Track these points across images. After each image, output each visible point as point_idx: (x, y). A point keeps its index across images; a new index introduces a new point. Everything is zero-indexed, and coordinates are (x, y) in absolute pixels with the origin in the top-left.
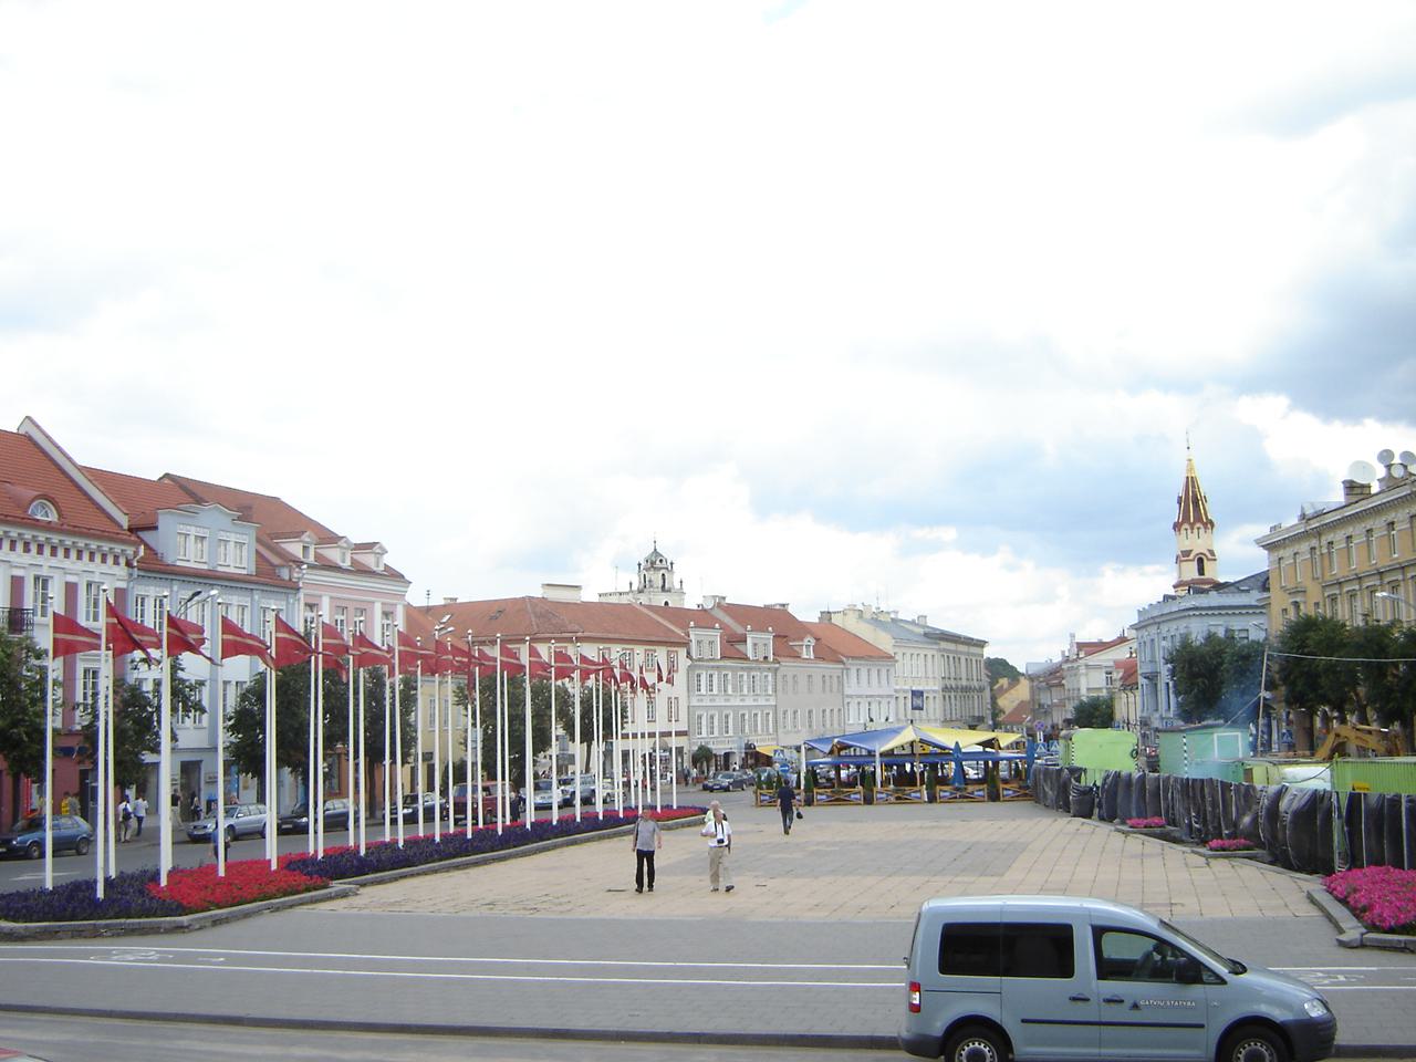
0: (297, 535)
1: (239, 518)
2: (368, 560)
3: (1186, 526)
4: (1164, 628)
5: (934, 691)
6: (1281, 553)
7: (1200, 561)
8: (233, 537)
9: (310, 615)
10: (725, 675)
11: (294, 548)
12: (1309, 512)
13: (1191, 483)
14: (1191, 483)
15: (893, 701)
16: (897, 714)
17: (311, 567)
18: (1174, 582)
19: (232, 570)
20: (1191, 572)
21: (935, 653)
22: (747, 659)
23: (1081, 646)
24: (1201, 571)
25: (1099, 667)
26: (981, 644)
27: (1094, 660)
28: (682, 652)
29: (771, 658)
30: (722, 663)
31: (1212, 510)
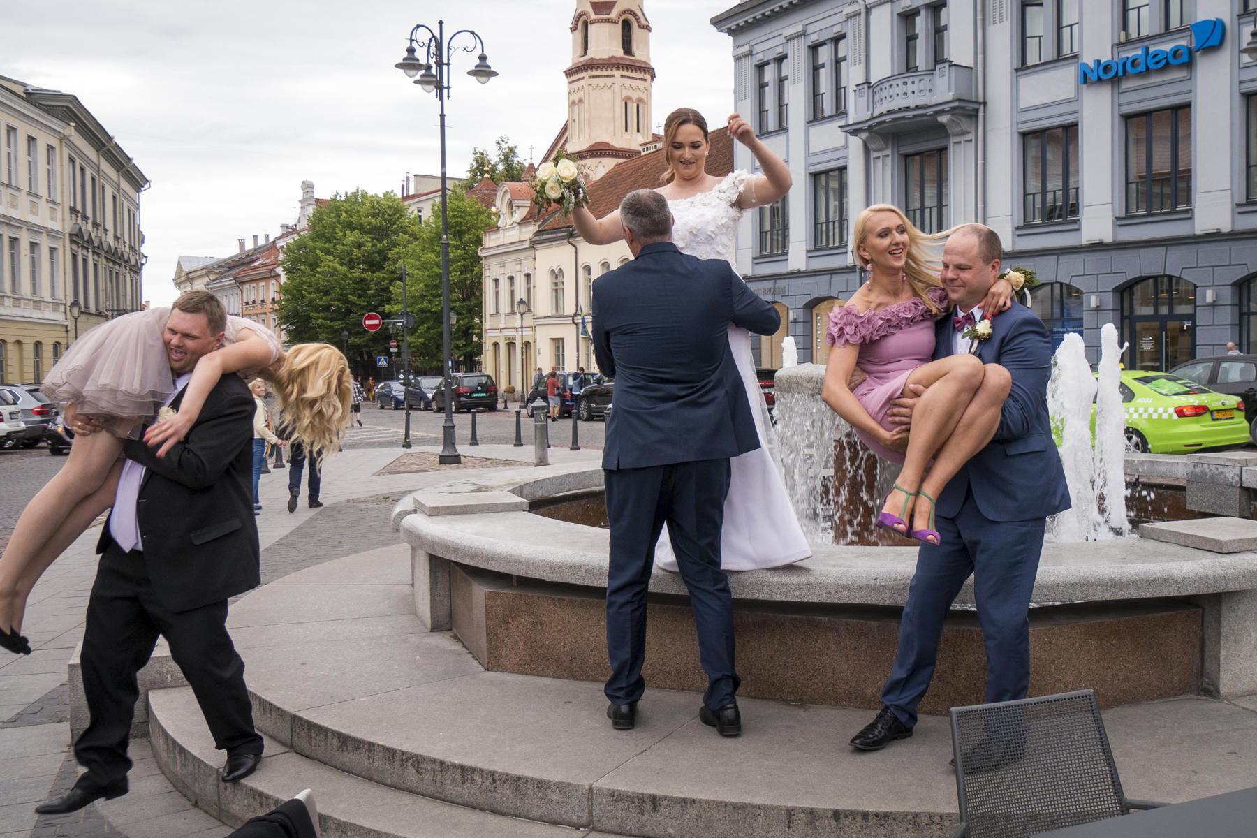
5: (51, 233)
7: (626, 26)
18: (568, 65)
20: (605, 42)
21: (54, 142)
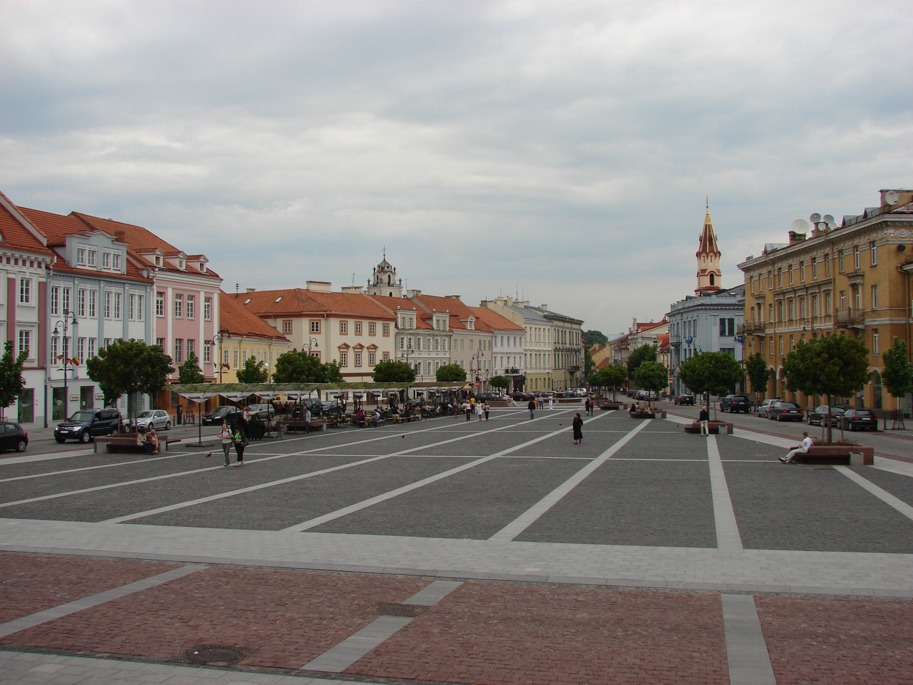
0: (152, 251)
1: (117, 240)
2: (196, 265)
3: (704, 254)
4: (685, 316)
6: (752, 274)
7: (712, 277)
8: (112, 252)
9: (160, 299)
10: (419, 339)
11: (151, 259)
12: (769, 249)
13: (708, 228)
14: (708, 228)
15: (523, 356)
16: (525, 364)
17: (161, 269)
18: (696, 288)
19: (112, 271)
20: (706, 282)
22: (433, 329)
23: (639, 325)
24: (712, 282)
25: (650, 338)
26: (580, 323)
27: (646, 334)
28: (392, 325)
29: (448, 329)
30: (417, 331)
31: (720, 245)
